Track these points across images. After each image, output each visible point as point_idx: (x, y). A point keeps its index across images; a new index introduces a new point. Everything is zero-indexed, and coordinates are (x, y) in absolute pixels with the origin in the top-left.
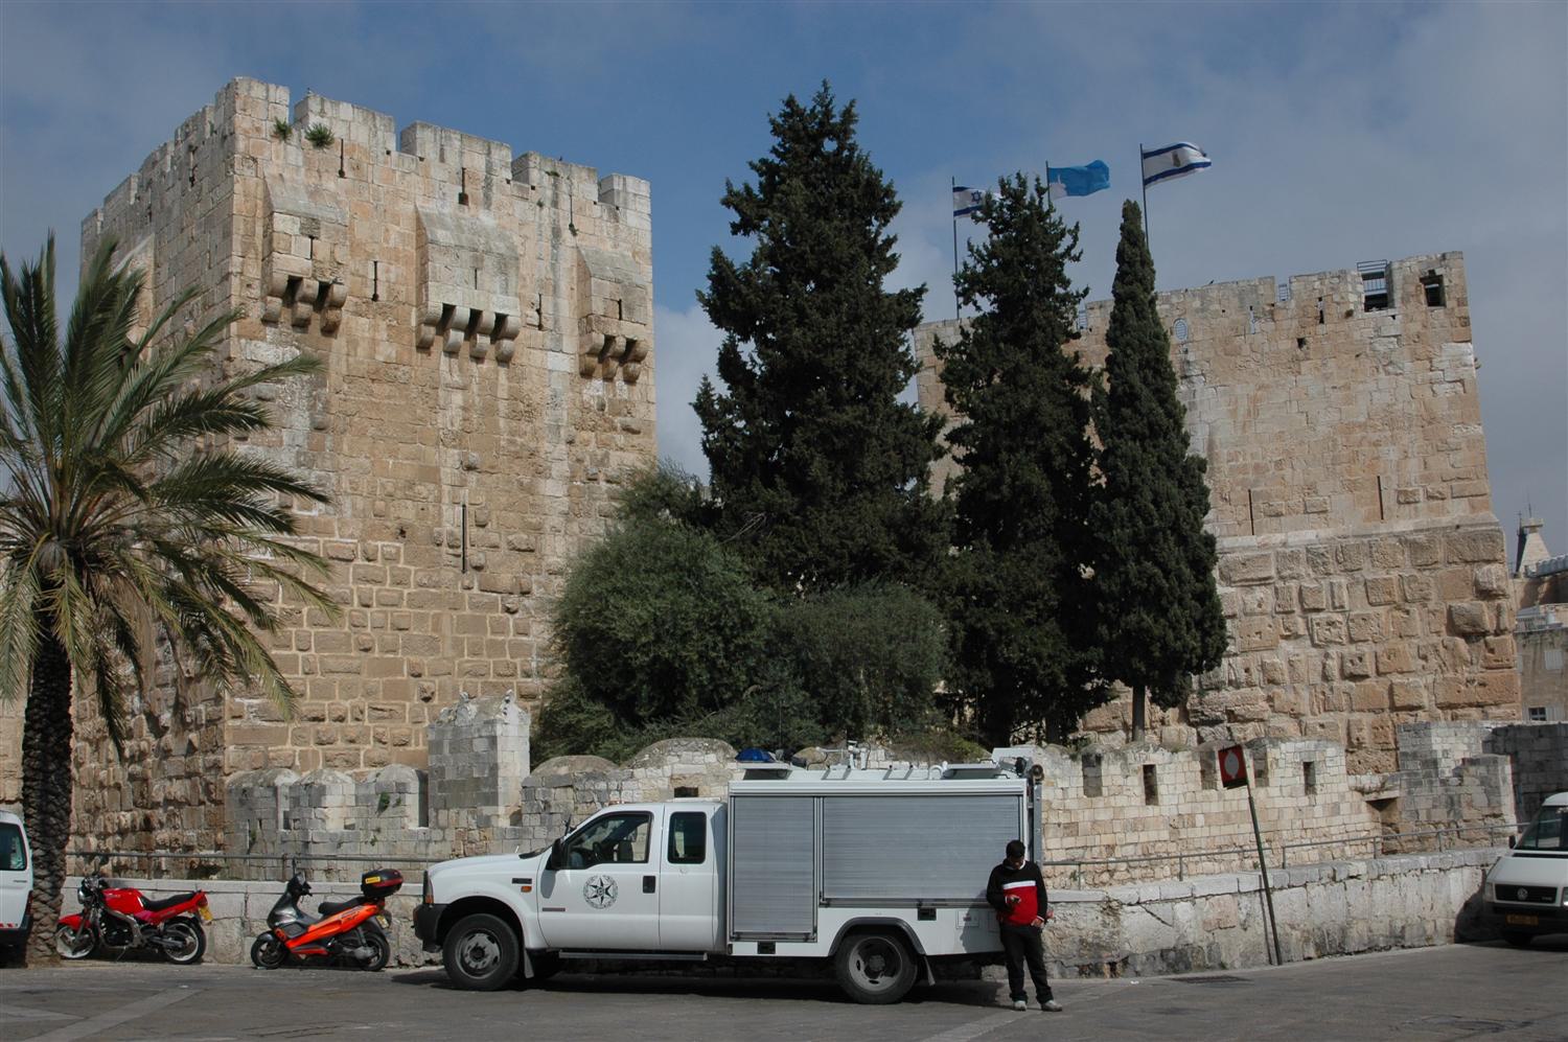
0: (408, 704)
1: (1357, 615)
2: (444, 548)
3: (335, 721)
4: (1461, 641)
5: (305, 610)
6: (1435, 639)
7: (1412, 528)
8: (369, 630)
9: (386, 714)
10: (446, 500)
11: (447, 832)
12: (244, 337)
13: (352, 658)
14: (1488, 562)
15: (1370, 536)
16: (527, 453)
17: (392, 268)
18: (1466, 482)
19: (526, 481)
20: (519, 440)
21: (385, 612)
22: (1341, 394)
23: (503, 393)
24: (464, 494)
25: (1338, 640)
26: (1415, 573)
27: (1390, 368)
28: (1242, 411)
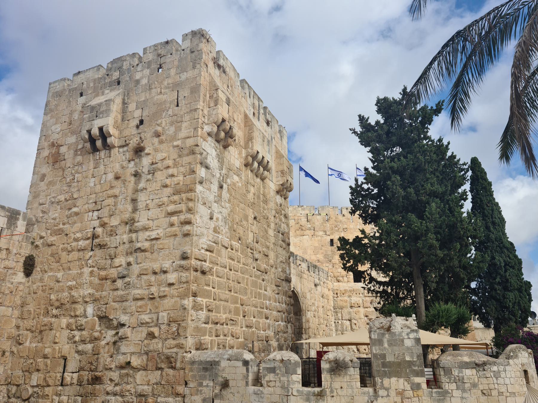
0: (239, 318)
2: (249, 250)
3: (220, 325)
5: (215, 269)
8: (231, 282)
9: (234, 323)
10: (249, 229)
11: (390, 390)
12: (203, 138)
13: (225, 294)
16: (266, 217)
17: (239, 131)
19: (266, 228)
20: (265, 212)
21: (235, 274)
23: (262, 192)
24: (254, 228)
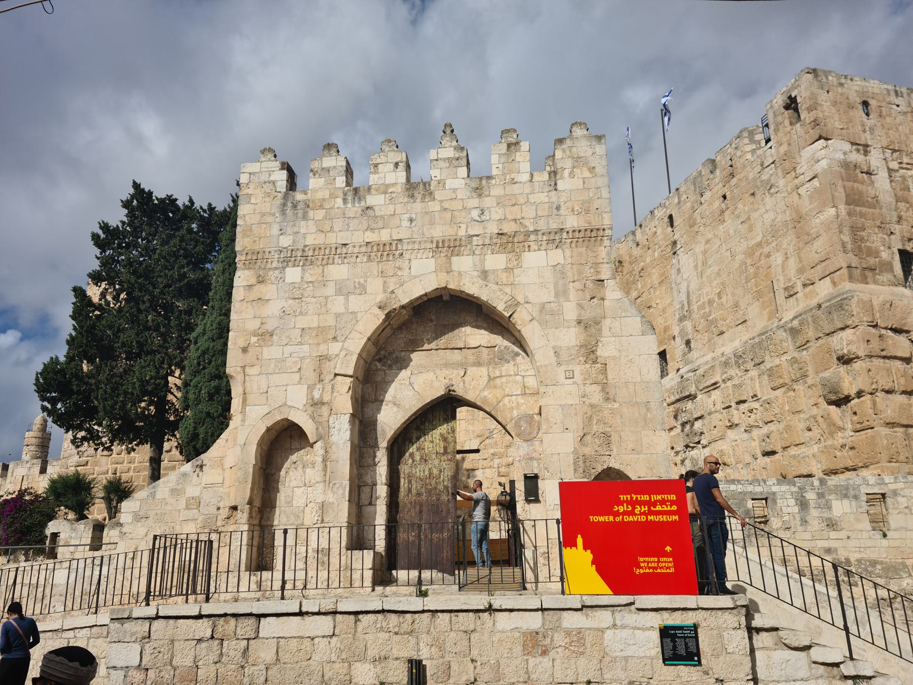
1: (764, 401)
4: (833, 408)
6: (815, 411)
7: (791, 318)
14: (842, 329)
15: (766, 332)
18: (827, 262)
22: (746, 226)
25: (756, 424)
26: (796, 354)
27: (772, 190)
28: (700, 264)
